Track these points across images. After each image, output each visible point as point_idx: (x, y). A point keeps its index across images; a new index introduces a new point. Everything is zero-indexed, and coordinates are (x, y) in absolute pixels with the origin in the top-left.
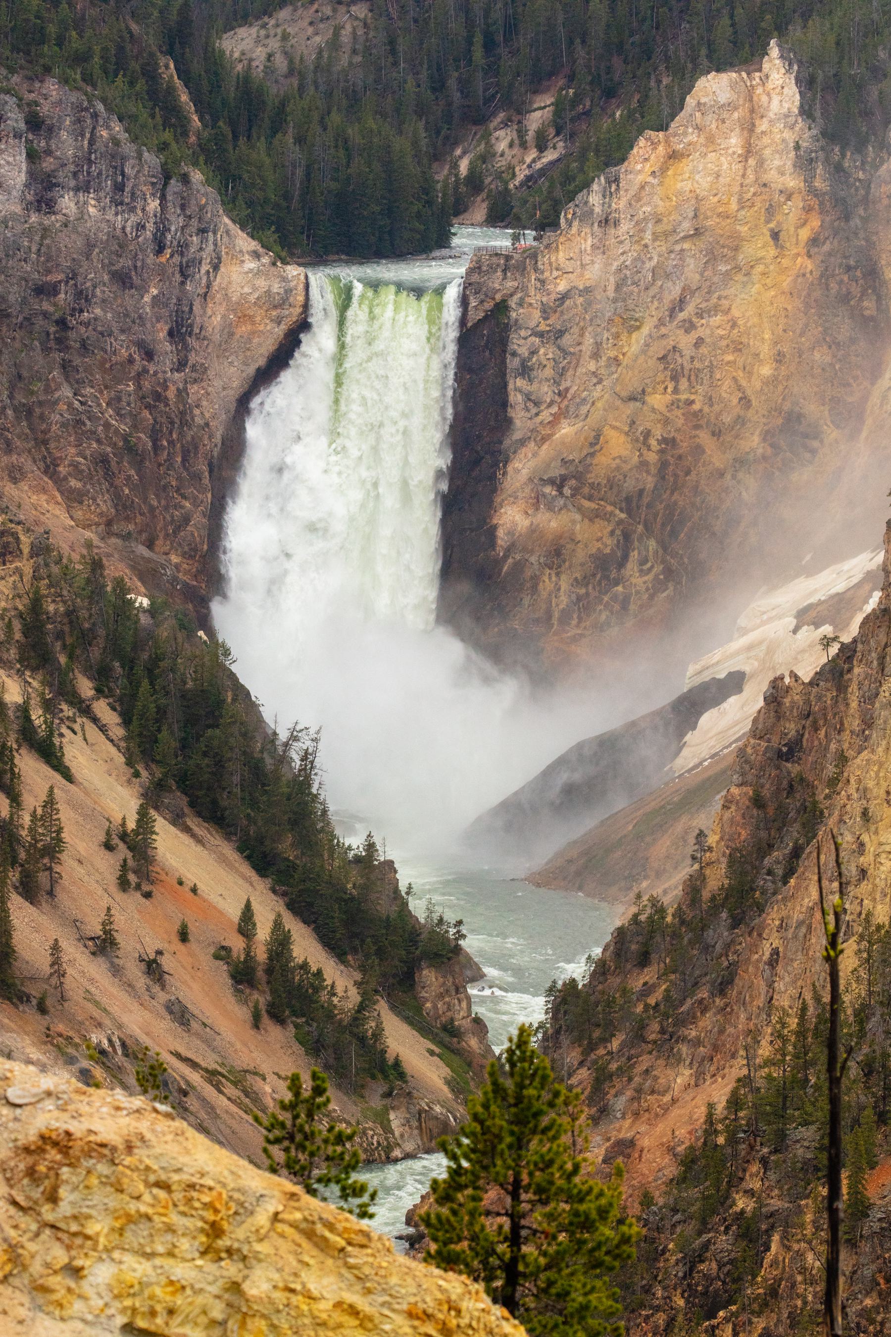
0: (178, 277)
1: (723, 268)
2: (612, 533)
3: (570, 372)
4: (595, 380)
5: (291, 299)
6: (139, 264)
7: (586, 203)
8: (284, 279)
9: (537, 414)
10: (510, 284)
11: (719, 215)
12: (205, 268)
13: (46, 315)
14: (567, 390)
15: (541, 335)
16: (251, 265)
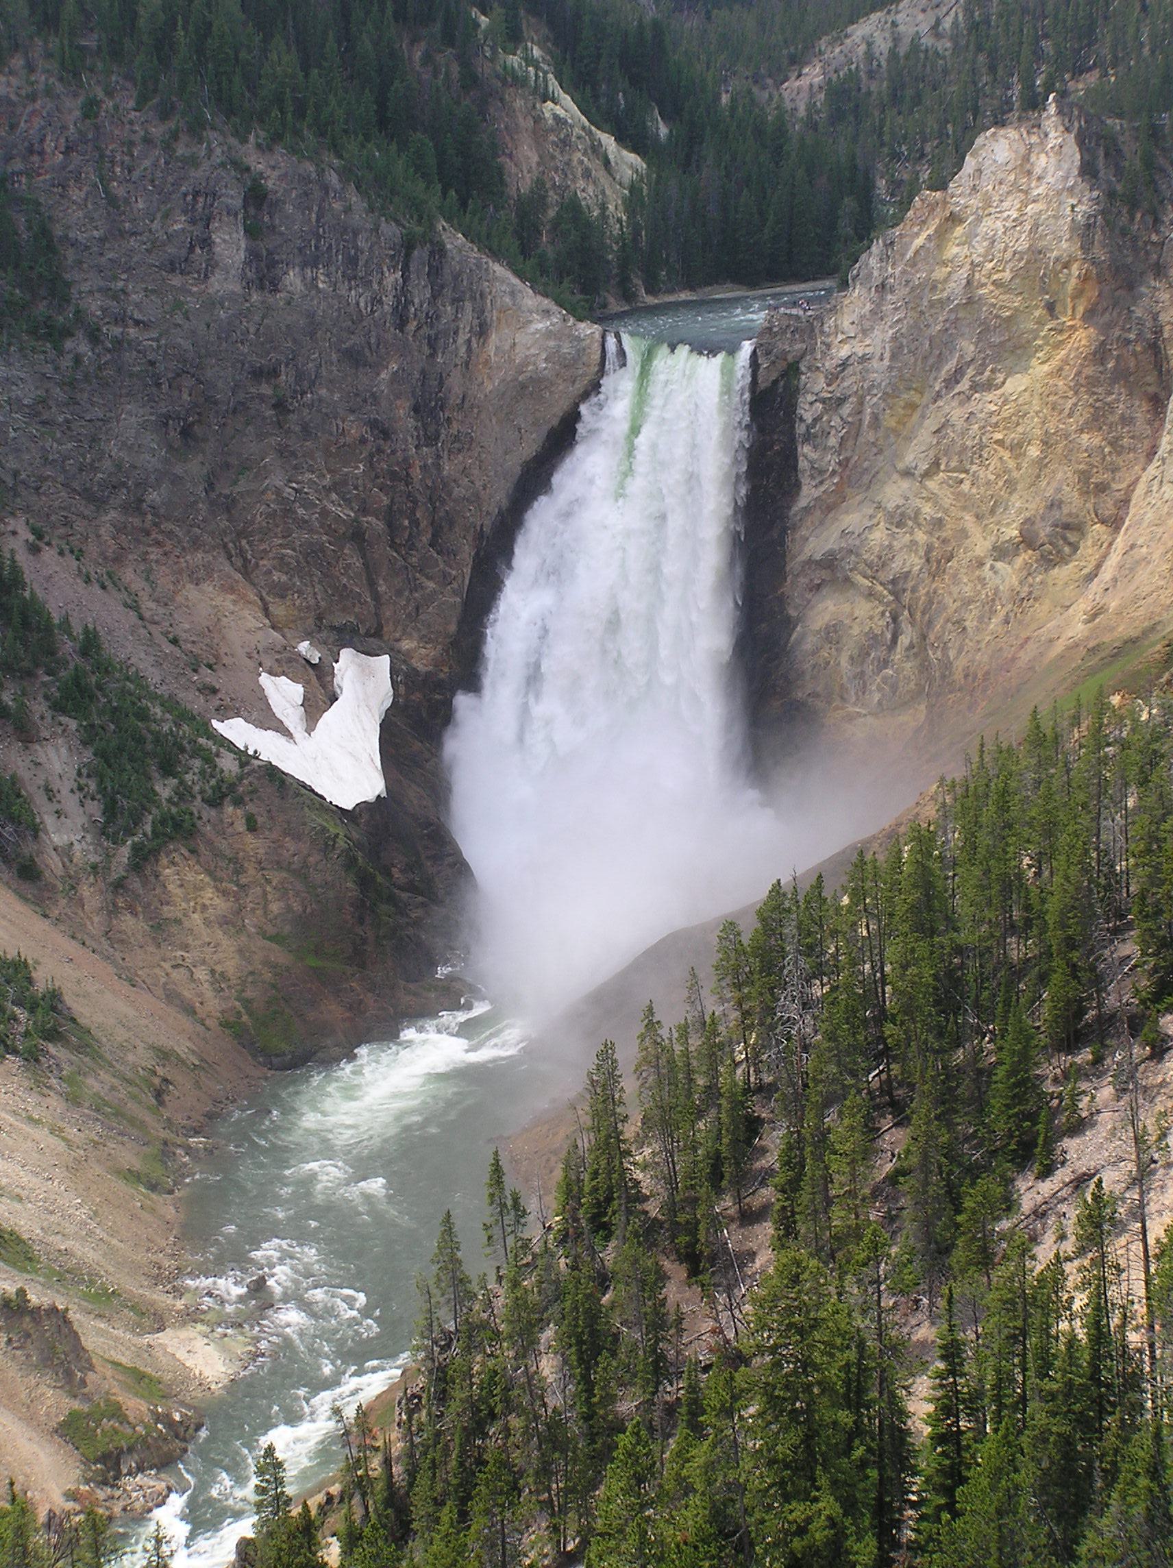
0: (426, 350)
1: (996, 339)
2: (883, 614)
3: (850, 443)
4: (875, 450)
5: (585, 359)
6: (373, 340)
7: (867, 265)
8: (578, 339)
9: (821, 483)
10: (799, 346)
11: (994, 283)
12: (462, 338)
13: (262, 398)
14: (848, 460)
15: (823, 401)
16: (540, 325)
